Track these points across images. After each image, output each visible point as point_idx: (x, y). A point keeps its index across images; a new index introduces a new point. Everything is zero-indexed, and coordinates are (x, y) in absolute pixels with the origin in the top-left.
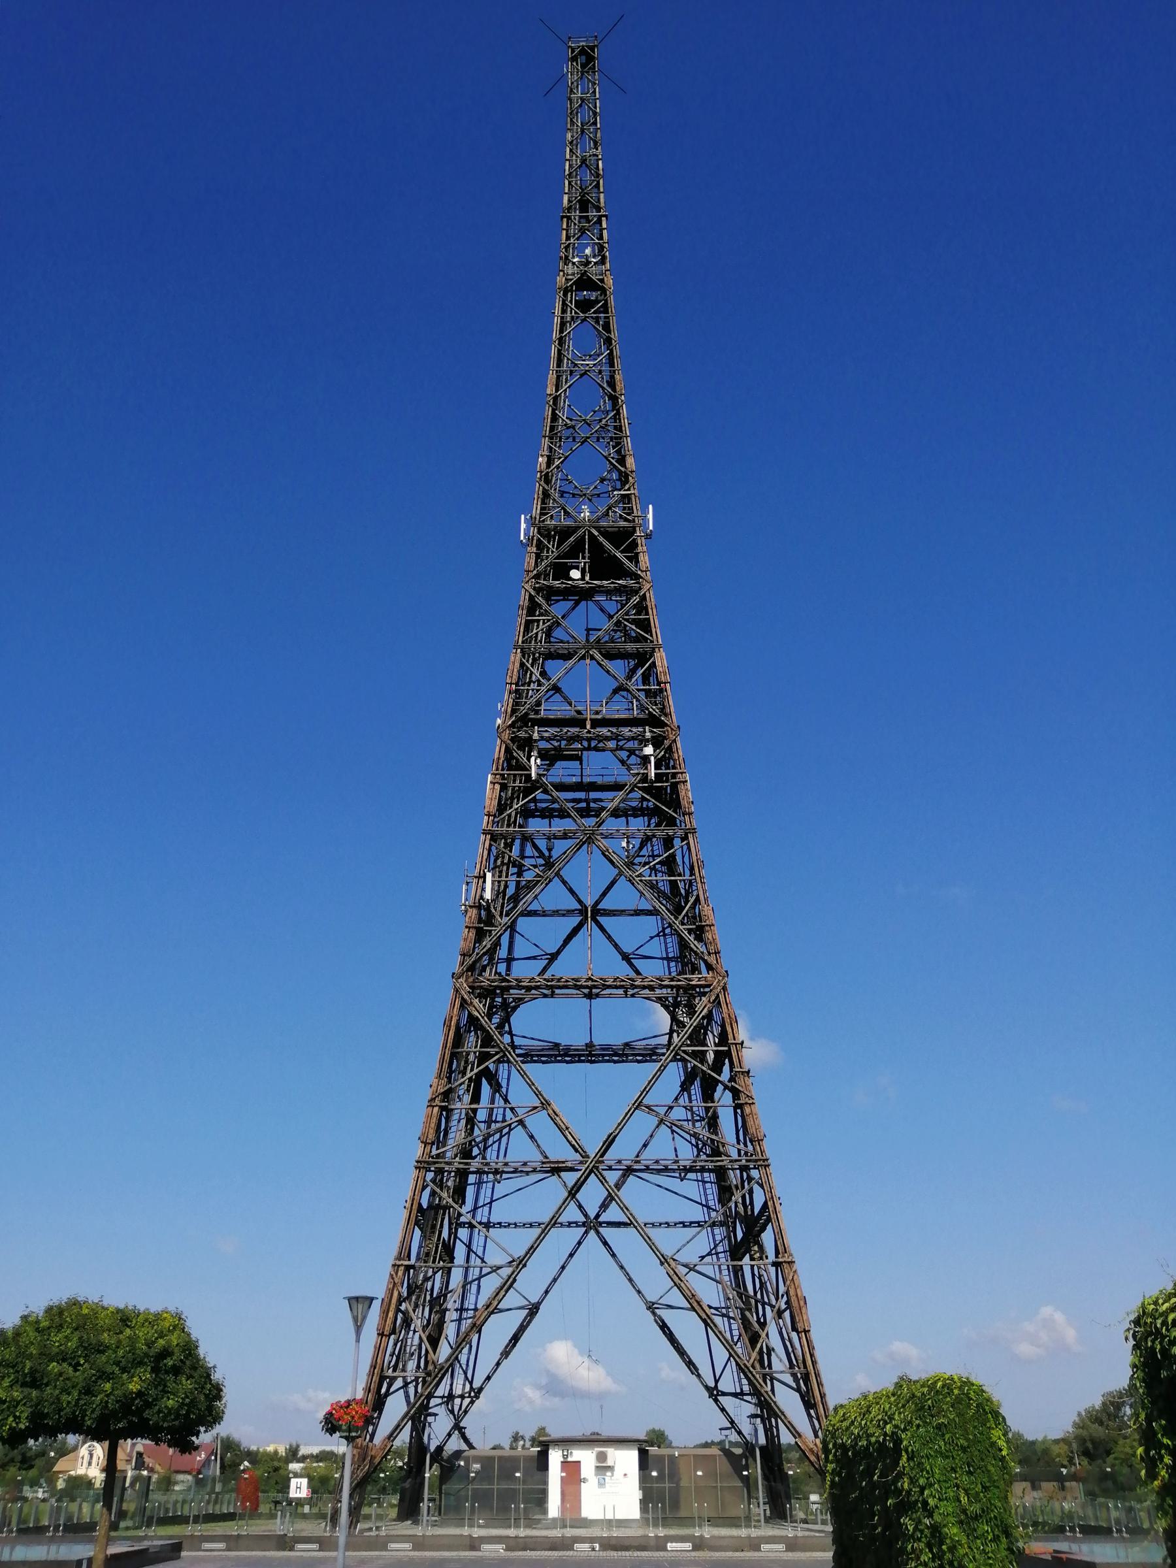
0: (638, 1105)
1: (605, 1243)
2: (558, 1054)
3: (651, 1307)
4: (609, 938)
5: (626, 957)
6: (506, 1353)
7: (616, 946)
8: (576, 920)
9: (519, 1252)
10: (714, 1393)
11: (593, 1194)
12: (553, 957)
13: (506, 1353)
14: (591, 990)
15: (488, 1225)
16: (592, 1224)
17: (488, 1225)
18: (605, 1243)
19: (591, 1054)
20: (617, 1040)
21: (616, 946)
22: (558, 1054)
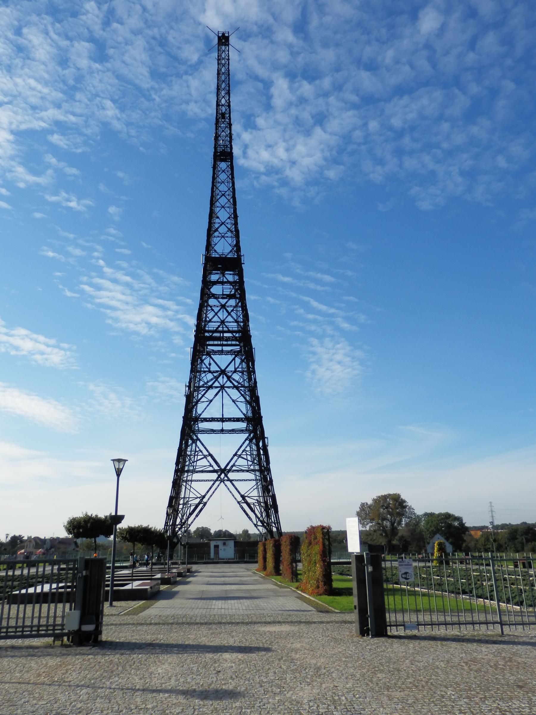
0: (235, 455)
1: (226, 486)
2: (213, 431)
3: (238, 502)
4: (228, 395)
5: (234, 401)
6: (197, 516)
7: (231, 398)
8: (219, 389)
9: (203, 494)
10: (256, 525)
11: (223, 476)
12: (211, 401)
13: (197, 516)
14: (222, 420)
15: (191, 481)
16: (222, 481)
17: (191, 481)
18: (226, 486)
19: (222, 431)
20: (231, 429)
21: (231, 398)
22: (213, 431)
